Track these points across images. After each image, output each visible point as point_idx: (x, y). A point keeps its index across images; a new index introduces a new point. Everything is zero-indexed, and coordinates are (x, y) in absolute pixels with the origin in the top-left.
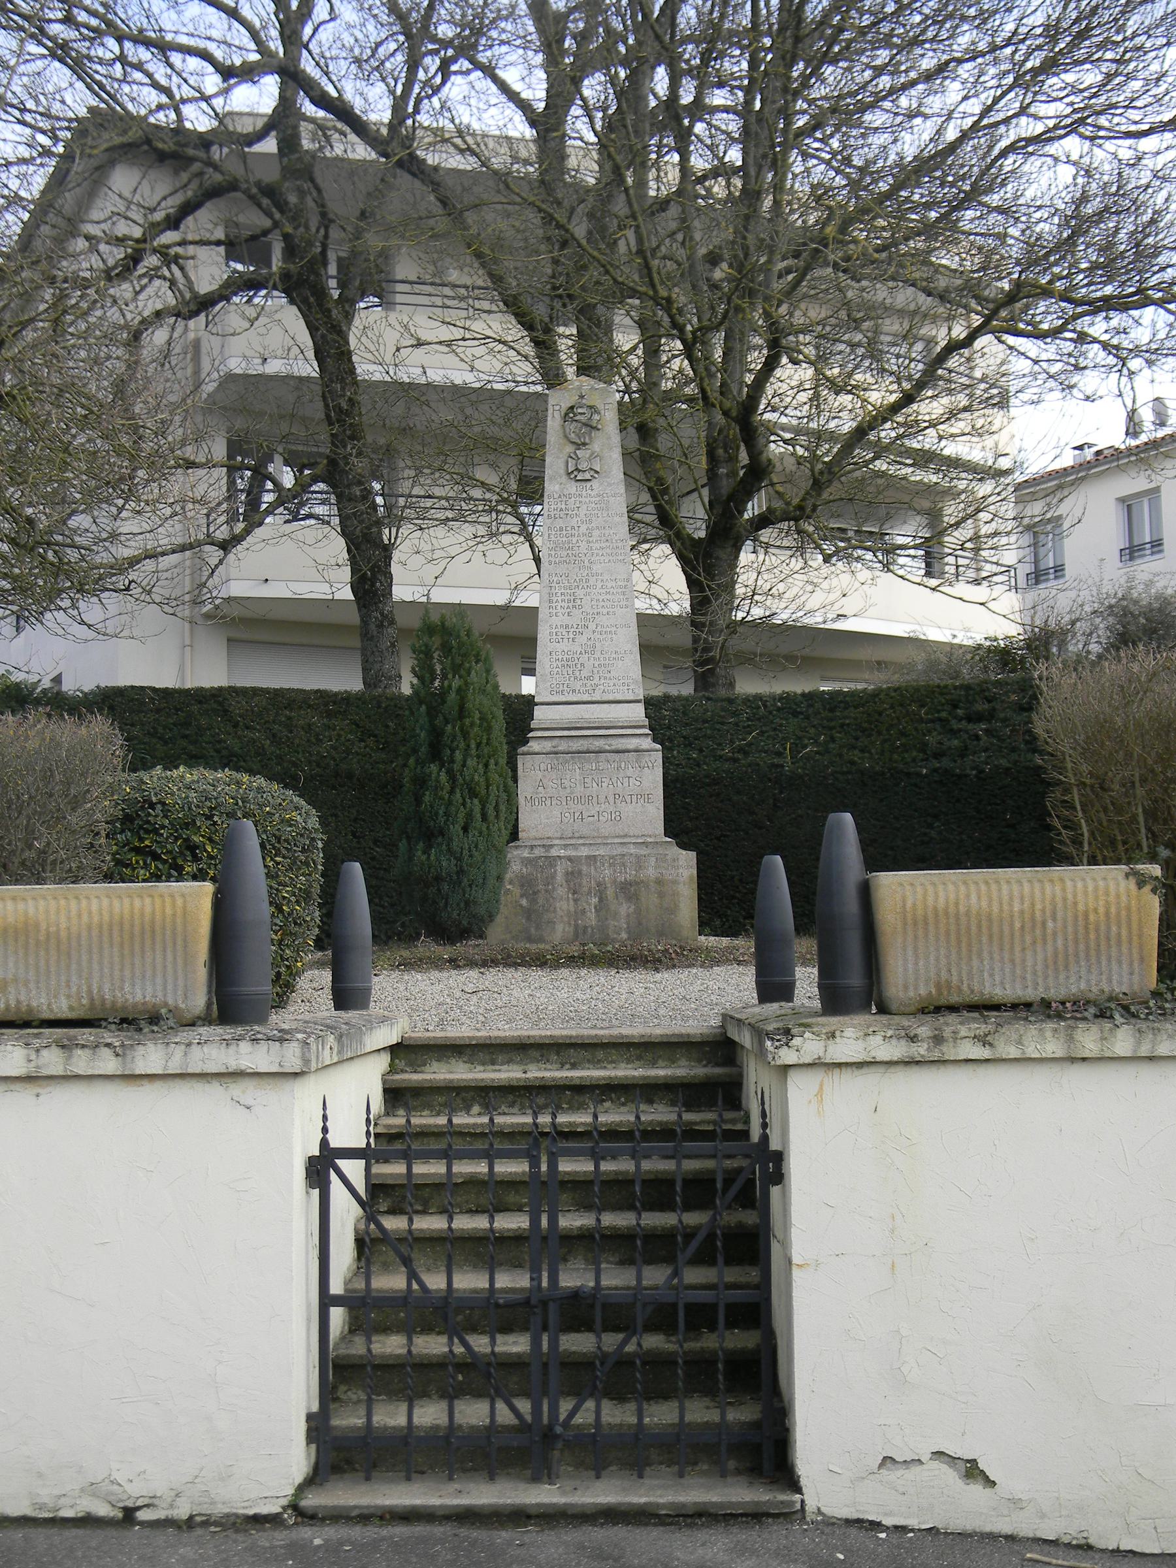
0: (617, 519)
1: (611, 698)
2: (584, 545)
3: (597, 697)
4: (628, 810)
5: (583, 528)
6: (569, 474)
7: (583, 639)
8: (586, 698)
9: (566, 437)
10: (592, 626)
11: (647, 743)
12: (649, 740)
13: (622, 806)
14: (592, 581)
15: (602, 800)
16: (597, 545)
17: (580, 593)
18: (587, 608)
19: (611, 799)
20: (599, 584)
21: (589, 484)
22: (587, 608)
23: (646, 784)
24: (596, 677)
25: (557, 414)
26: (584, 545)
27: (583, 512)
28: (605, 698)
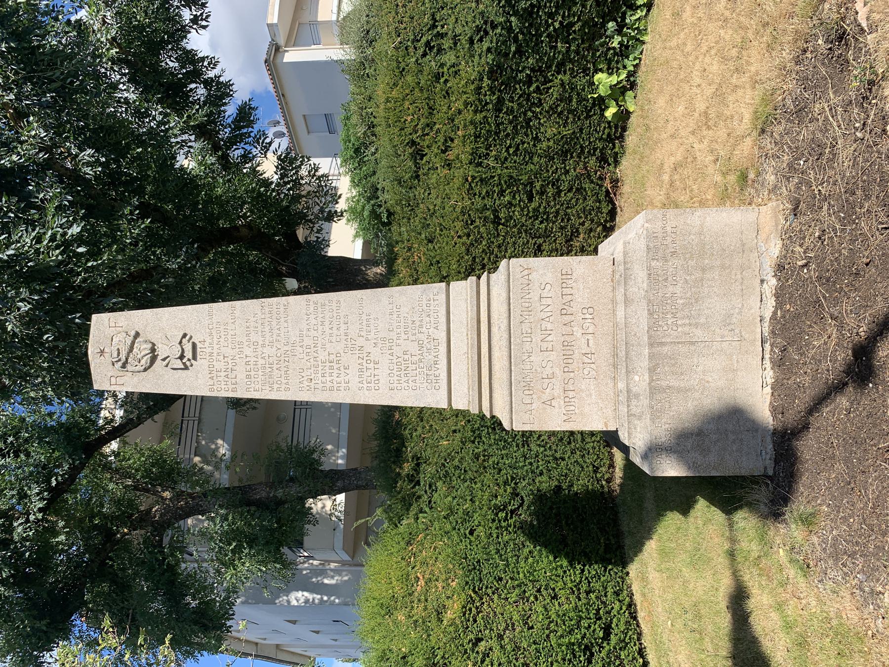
0: (237, 313)
1: (443, 320)
2: (267, 351)
3: (444, 335)
4: (581, 296)
5: (248, 351)
6: (186, 368)
7: (375, 354)
8: (443, 349)
9: (145, 370)
10: (361, 342)
11: (498, 277)
12: (493, 276)
13: (576, 308)
14: (307, 341)
15: (568, 329)
16: (268, 335)
17: (323, 355)
18: (340, 348)
19: (567, 319)
20: (313, 333)
21: (199, 345)
22: (340, 348)
23: (549, 277)
24: (421, 336)
25: (120, 381)
26: (267, 351)
27: (229, 352)
28: (444, 327)
